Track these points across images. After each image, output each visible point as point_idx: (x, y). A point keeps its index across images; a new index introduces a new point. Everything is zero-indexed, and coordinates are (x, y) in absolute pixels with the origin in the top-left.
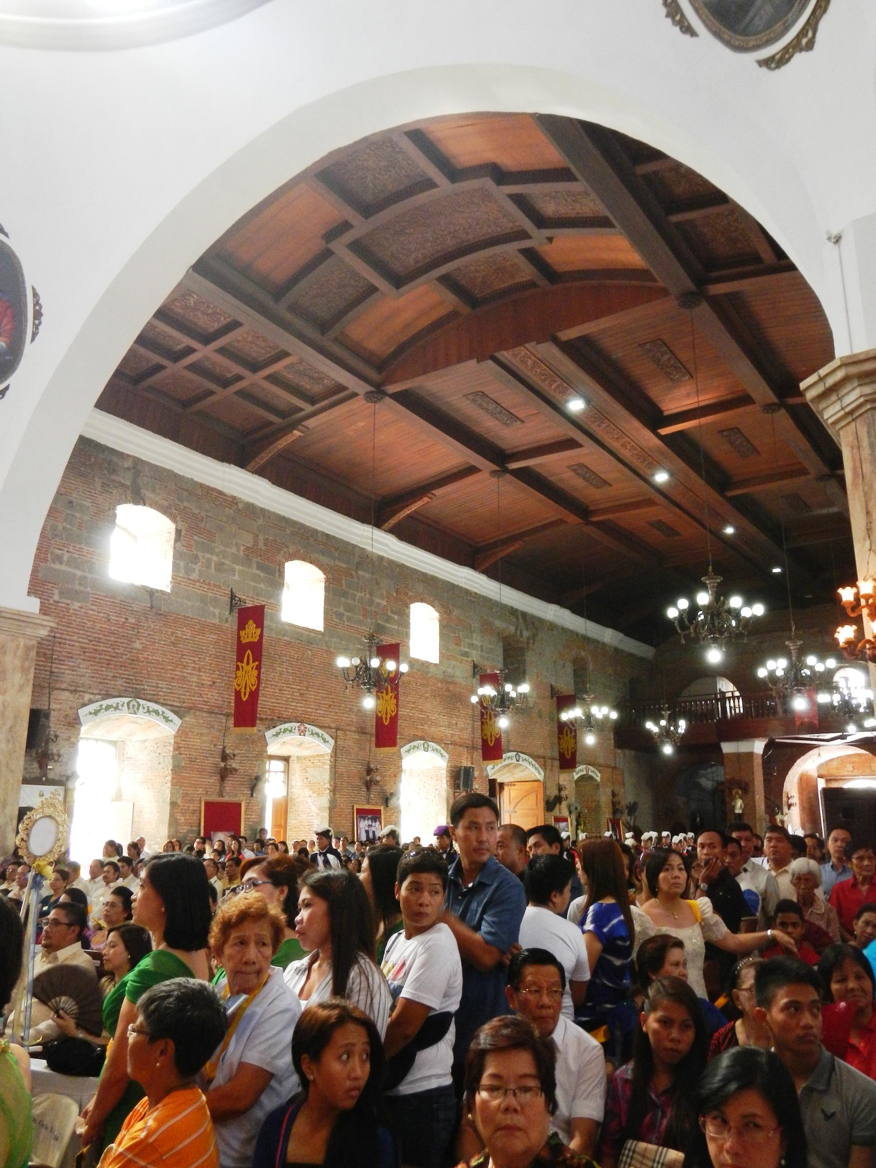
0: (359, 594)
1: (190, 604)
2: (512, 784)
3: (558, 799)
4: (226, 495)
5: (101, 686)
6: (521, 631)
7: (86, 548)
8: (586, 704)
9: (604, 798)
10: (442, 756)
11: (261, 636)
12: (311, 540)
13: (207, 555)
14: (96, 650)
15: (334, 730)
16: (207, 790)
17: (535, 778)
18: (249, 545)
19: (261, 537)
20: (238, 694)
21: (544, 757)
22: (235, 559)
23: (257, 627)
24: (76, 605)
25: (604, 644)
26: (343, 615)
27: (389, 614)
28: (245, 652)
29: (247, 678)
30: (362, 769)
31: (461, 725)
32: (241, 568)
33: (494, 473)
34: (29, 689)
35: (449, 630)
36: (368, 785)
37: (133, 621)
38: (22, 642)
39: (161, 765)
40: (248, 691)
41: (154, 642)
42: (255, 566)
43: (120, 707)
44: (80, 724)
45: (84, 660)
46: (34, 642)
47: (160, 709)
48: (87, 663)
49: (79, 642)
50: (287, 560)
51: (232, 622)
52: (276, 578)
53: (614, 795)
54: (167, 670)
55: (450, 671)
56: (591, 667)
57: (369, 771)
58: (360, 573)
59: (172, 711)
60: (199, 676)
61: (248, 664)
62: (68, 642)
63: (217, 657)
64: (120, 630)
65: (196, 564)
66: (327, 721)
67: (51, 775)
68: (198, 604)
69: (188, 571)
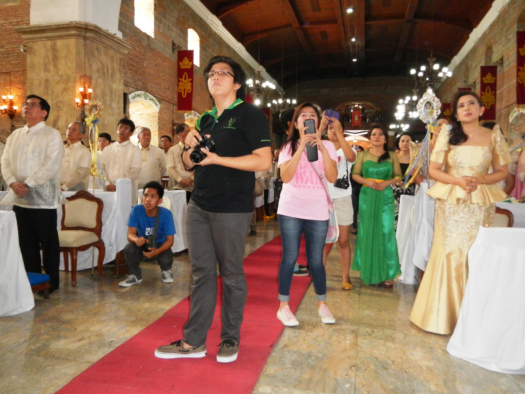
0: (209, 50)
5: (135, 84)
19: (181, 14)
20: (180, 95)
34: (122, 82)
40: (186, 93)
51: (174, 58)
58: (210, 39)
61: (185, 79)
68: (162, 46)
69: (159, 27)
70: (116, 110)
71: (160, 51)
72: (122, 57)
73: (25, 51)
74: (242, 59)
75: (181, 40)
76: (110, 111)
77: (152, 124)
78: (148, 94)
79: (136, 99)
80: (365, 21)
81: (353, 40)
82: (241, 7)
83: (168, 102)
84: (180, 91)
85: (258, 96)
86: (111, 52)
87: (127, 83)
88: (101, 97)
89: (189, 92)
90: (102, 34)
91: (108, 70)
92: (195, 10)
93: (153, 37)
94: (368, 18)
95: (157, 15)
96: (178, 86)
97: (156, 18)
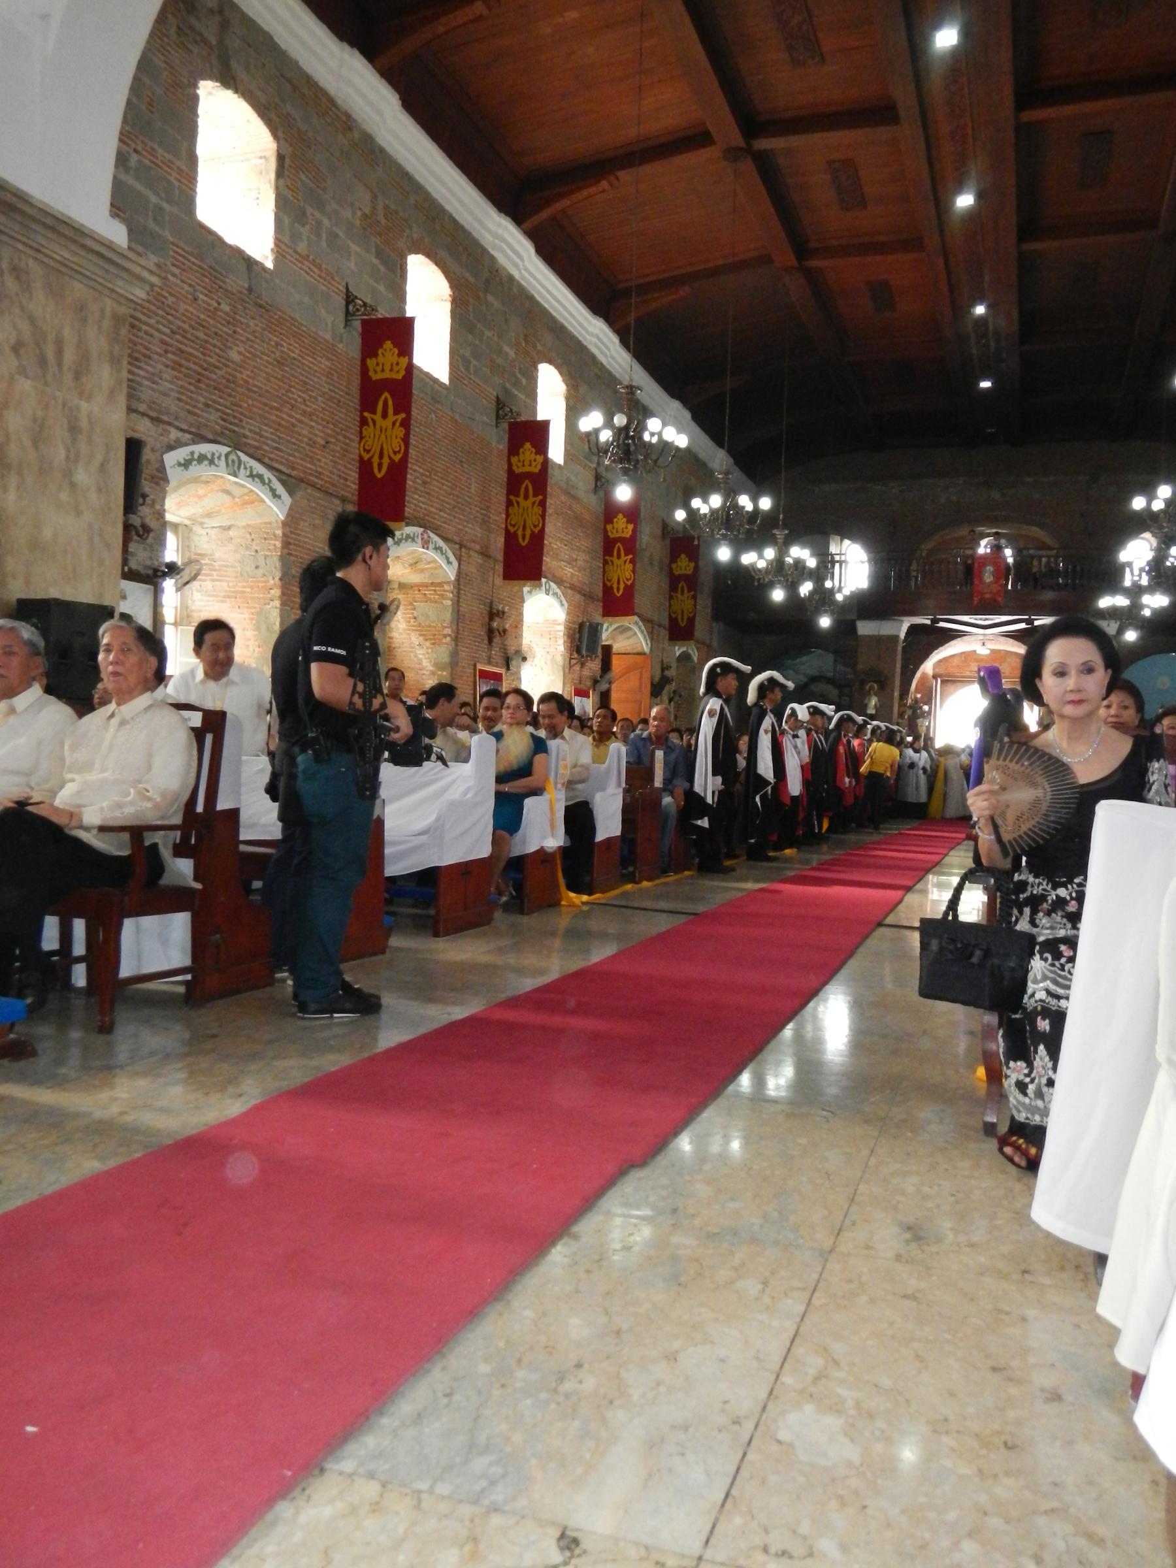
0: (488, 333)
1: (297, 296)
4: (338, 109)
5: (191, 418)
7: (160, 151)
10: (562, 605)
13: (317, 214)
14: (182, 351)
15: (457, 546)
17: (639, 650)
18: (367, 210)
19: (380, 202)
20: (365, 467)
23: (399, 355)
28: (380, 396)
29: (383, 436)
30: (484, 609)
31: (580, 563)
32: (358, 249)
33: (732, 154)
34: (122, 399)
36: (491, 634)
37: (227, 309)
39: (261, 571)
40: (386, 461)
41: (255, 355)
42: (373, 250)
43: (216, 461)
44: (166, 480)
45: (167, 366)
47: (267, 474)
48: (169, 370)
49: (158, 330)
51: (351, 345)
54: (272, 408)
57: (493, 614)
58: (490, 298)
59: (280, 480)
60: (311, 427)
61: (385, 415)
62: (144, 327)
64: (212, 322)
65: (303, 225)
68: (306, 299)
69: (295, 237)
70: (93, 496)
71: (297, 316)
72: (123, 310)
74: (610, 373)
75: (382, 288)
76: (64, 496)
77: (261, 562)
79: (195, 469)
80: (1021, 239)
81: (980, 310)
82: (593, 190)
83: (327, 492)
84: (366, 457)
86: (77, 289)
87: (160, 412)
88: (28, 443)
89: (397, 458)
90: (34, 219)
91: (59, 352)
92: (434, 194)
93: (269, 264)
94: (1028, 229)
95: (286, 192)
96: (361, 438)
97: (283, 204)
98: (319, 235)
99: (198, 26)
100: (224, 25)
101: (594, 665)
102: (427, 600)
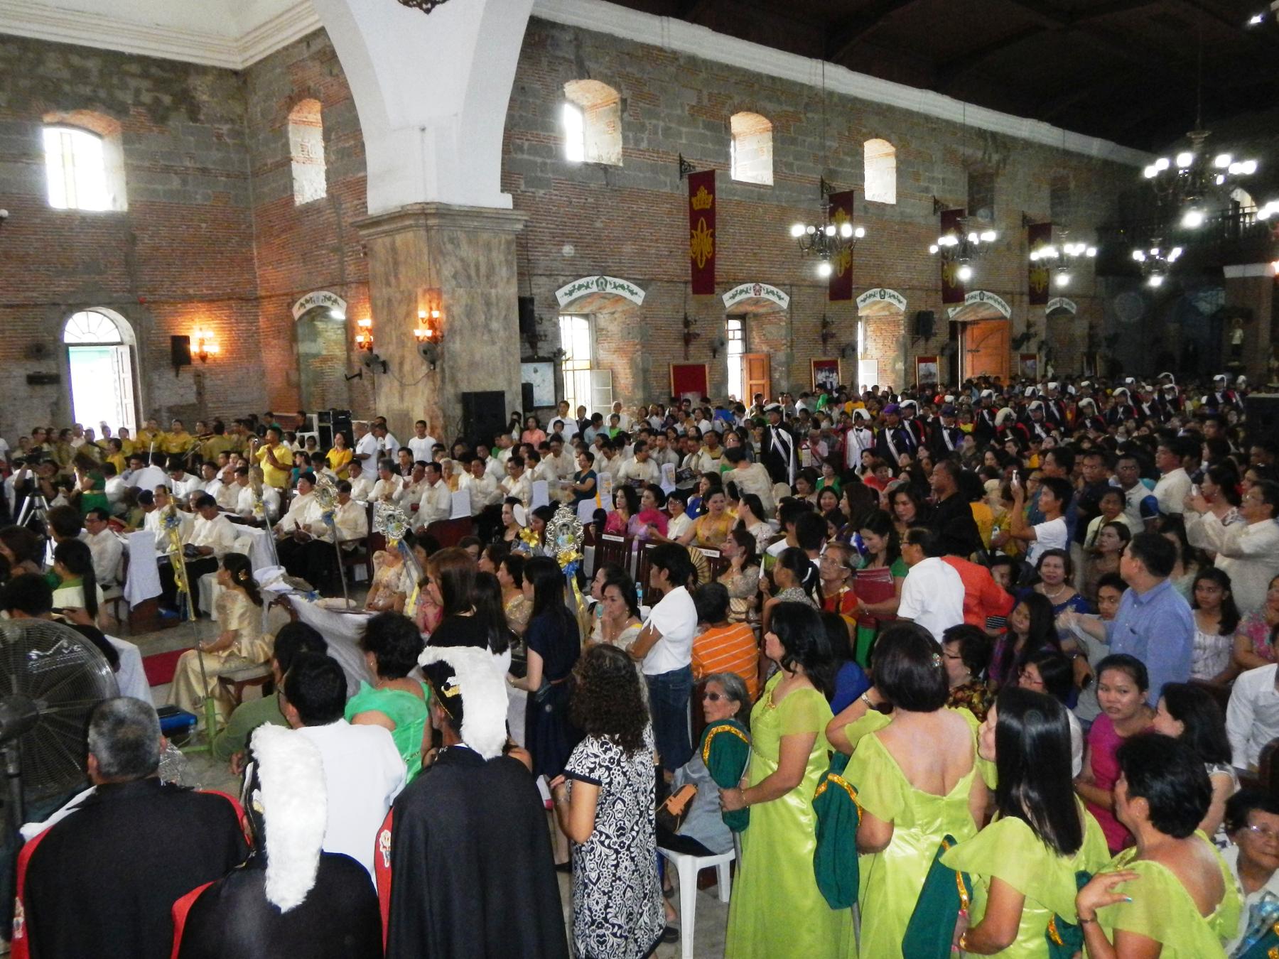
0: (809, 139)
2: (974, 323)
3: (1026, 337)
5: (571, 268)
6: (990, 158)
8: (1059, 242)
9: (1080, 329)
11: (714, 199)
12: (756, 87)
13: (654, 122)
16: (674, 355)
19: (705, 92)
20: (694, 263)
21: (1012, 293)
22: (681, 121)
24: (541, 192)
25: (1090, 158)
26: (792, 164)
27: (841, 156)
34: (515, 281)
35: (904, 171)
36: (825, 338)
38: (504, 237)
46: (512, 237)
47: (625, 283)
50: (733, 113)
51: (684, 187)
52: (723, 136)
53: (1091, 327)
55: (908, 210)
56: (1072, 185)
58: (810, 115)
63: (672, 226)
66: (782, 279)
67: (541, 353)
68: (649, 174)
69: (637, 141)
70: (502, 333)
72: (509, 238)
73: (365, 254)
75: (710, 145)
78: (608, 278)
85: (825, 257)
86: (485, 236)
91: (478, 270)
98: (656, 133)
99: (560, 54)
100: (579, 46)
101: (942, 336)
102: (771, 323)
